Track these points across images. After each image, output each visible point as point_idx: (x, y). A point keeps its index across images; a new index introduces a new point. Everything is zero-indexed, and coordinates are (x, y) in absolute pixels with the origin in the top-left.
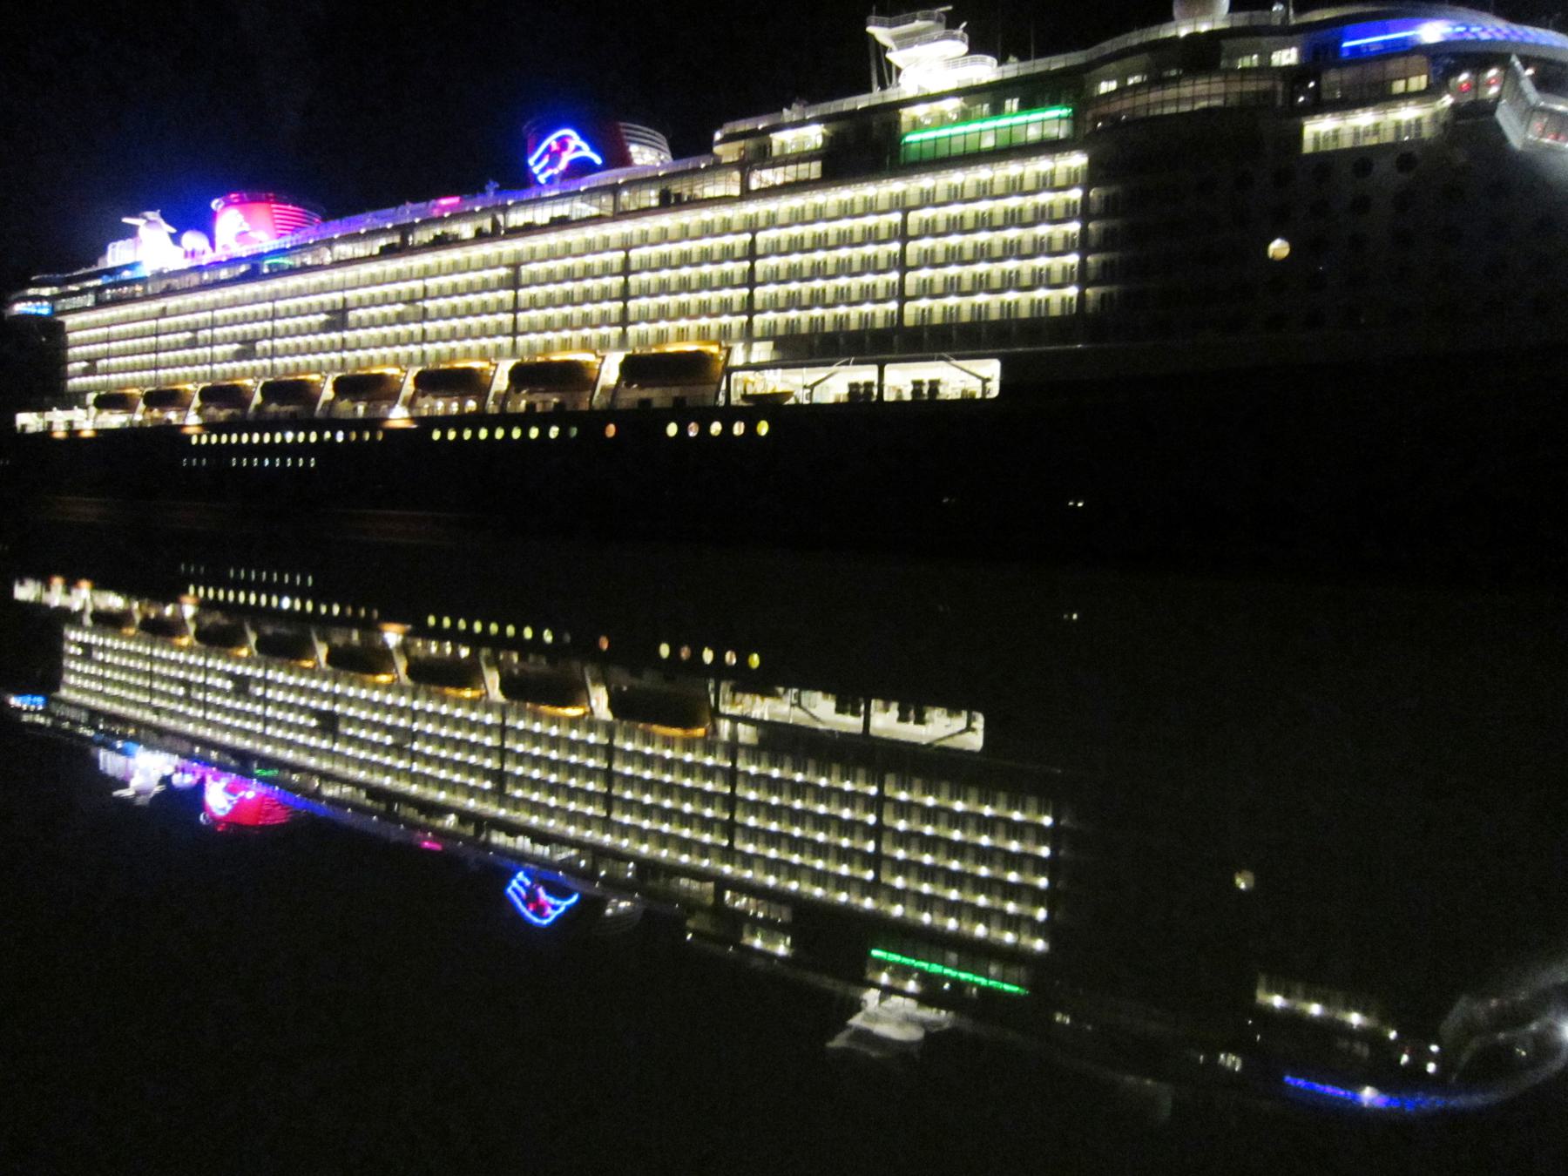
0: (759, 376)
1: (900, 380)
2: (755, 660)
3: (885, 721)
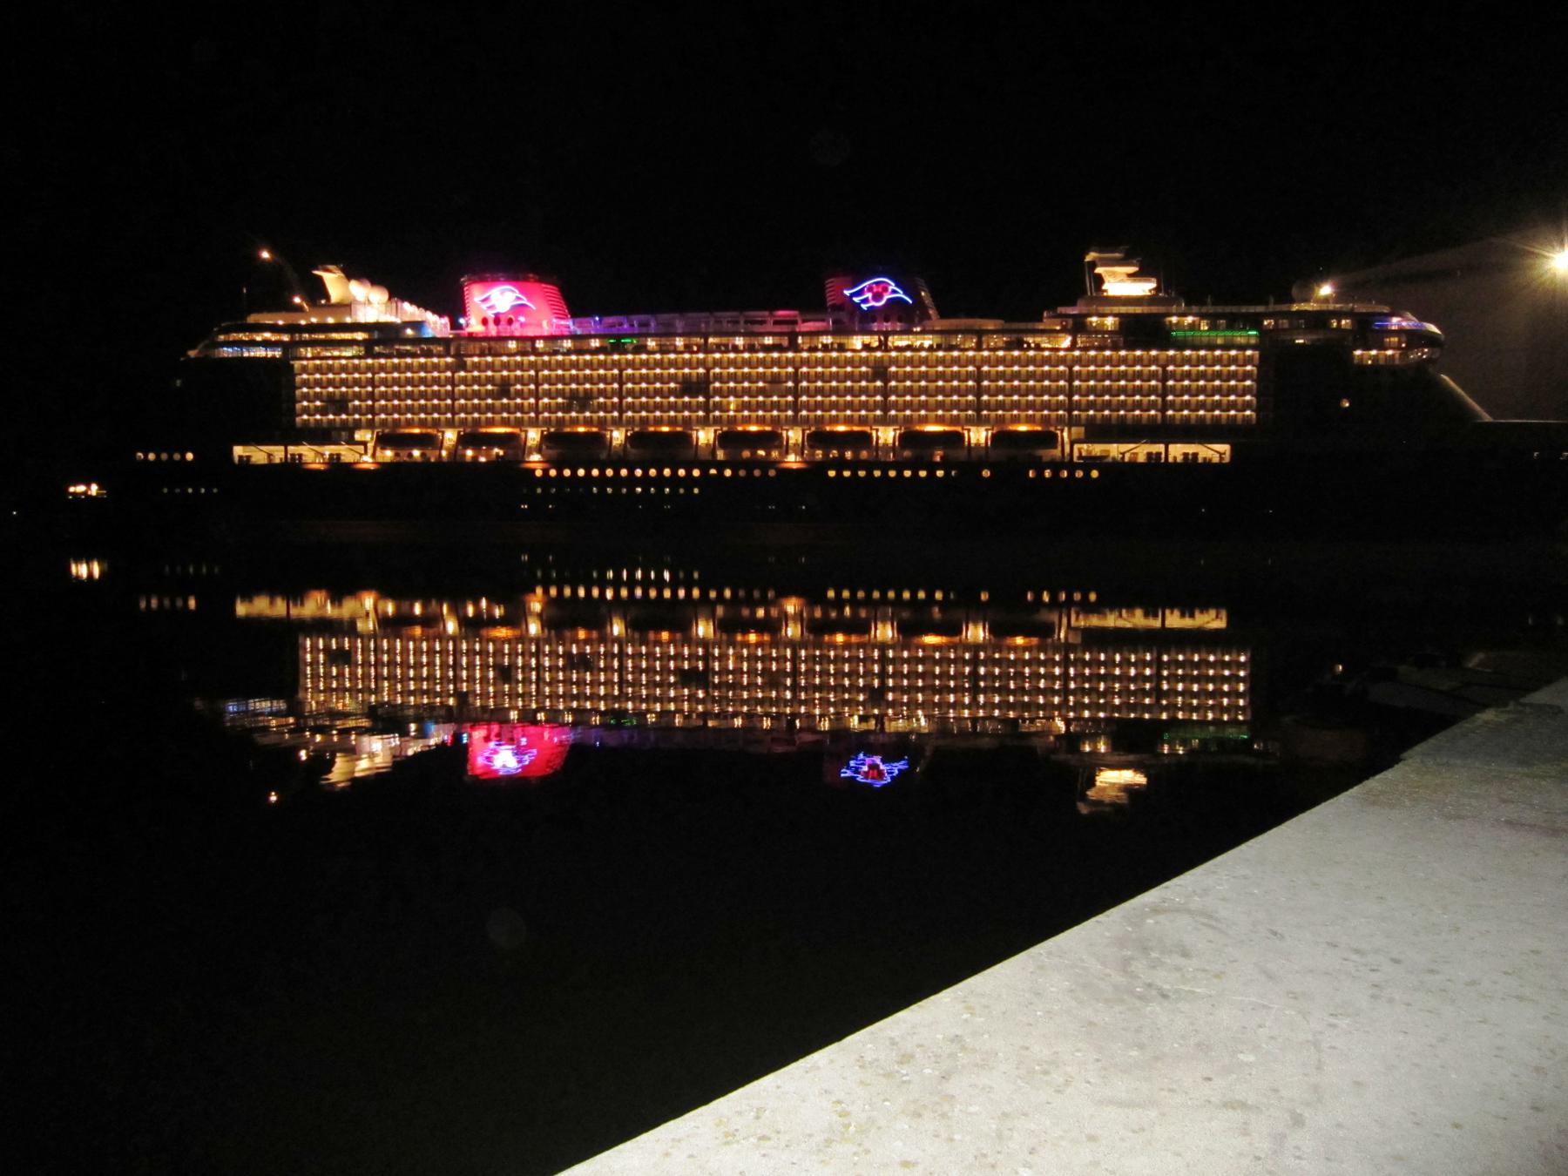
0: (1071, 444)
1: (1177, 451)
2: (1093, 597)
3: (1174, 620)
